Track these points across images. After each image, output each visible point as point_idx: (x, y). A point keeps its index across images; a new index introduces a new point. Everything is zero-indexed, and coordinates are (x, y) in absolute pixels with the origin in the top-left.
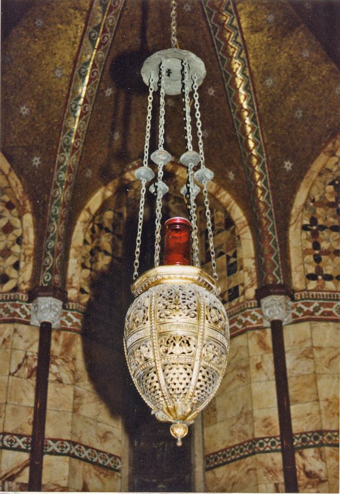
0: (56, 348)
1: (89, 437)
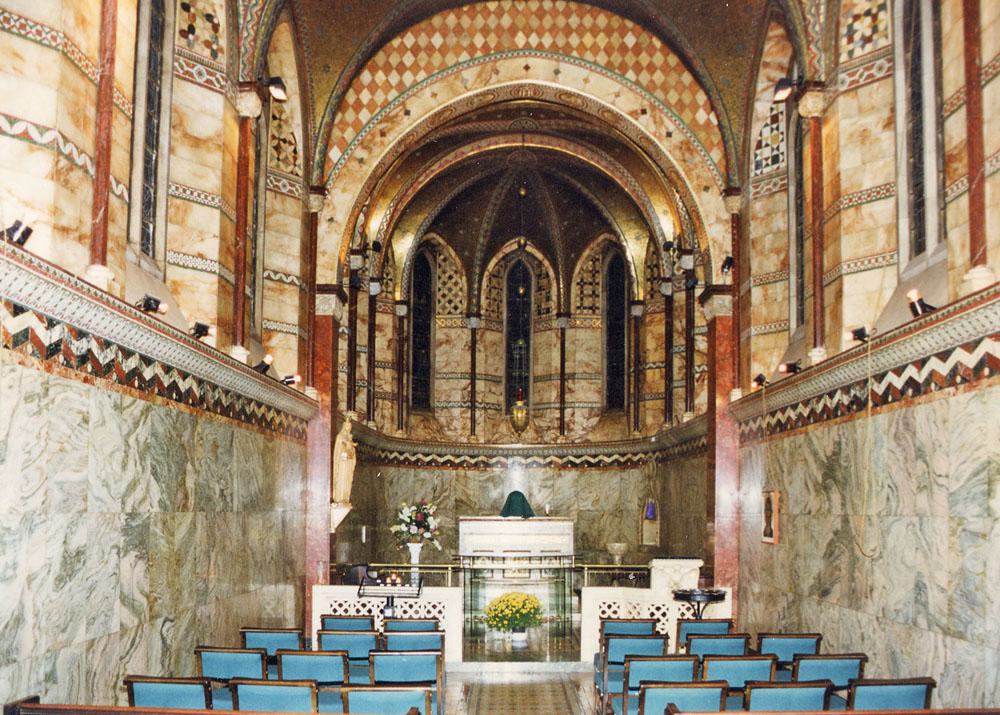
0: (478, 337)
1: (491, 371)
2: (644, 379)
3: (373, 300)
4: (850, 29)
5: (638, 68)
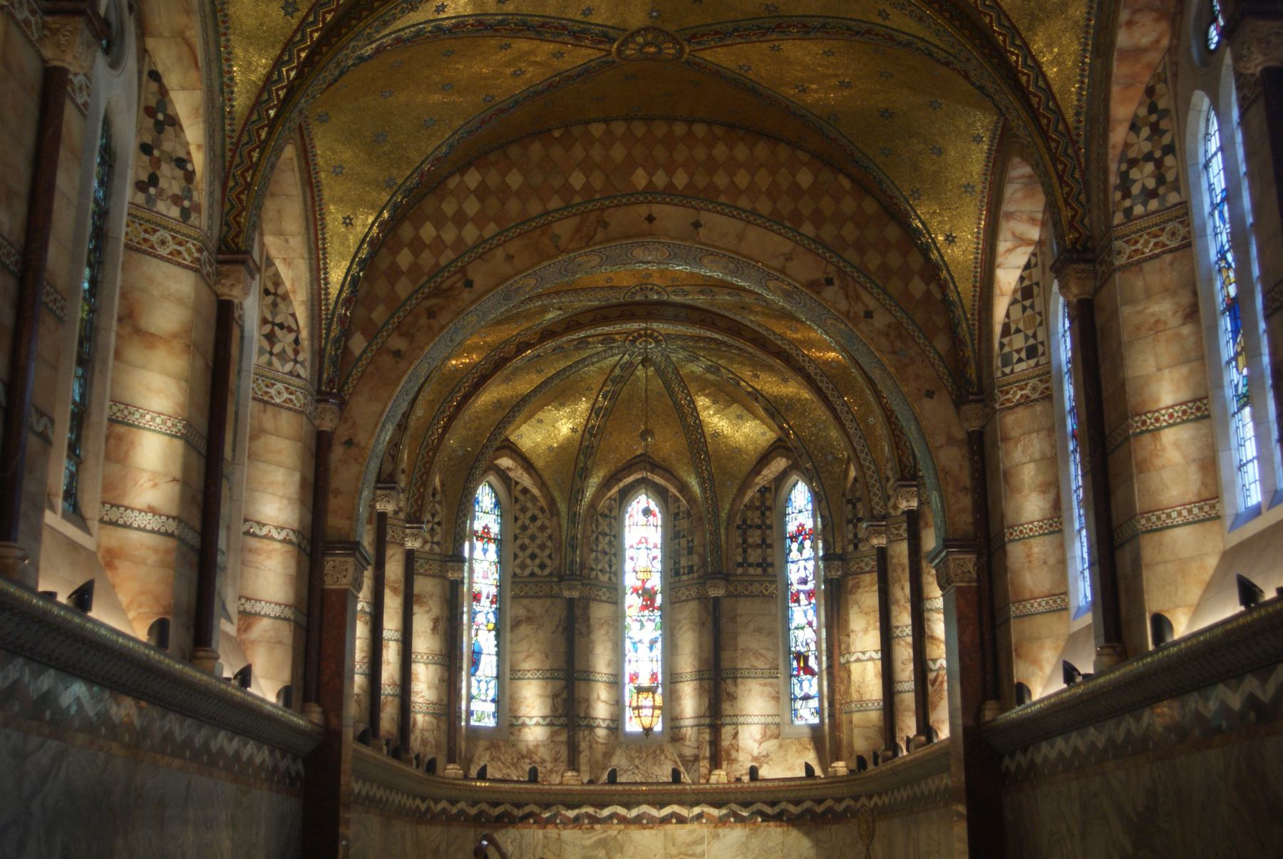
0: (578, 613)
2: (849, 677)
3: (410, 556)
4: (1124, 176)
5: (818, 218)
